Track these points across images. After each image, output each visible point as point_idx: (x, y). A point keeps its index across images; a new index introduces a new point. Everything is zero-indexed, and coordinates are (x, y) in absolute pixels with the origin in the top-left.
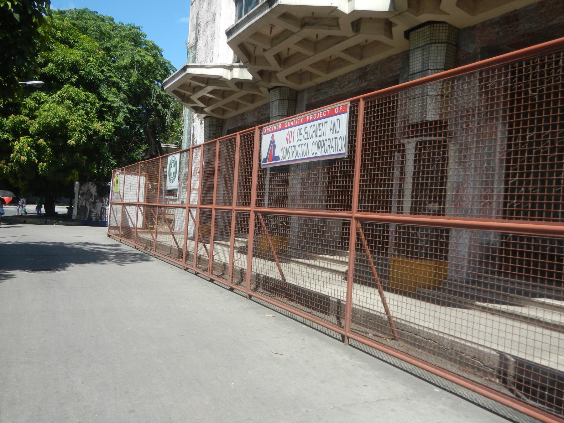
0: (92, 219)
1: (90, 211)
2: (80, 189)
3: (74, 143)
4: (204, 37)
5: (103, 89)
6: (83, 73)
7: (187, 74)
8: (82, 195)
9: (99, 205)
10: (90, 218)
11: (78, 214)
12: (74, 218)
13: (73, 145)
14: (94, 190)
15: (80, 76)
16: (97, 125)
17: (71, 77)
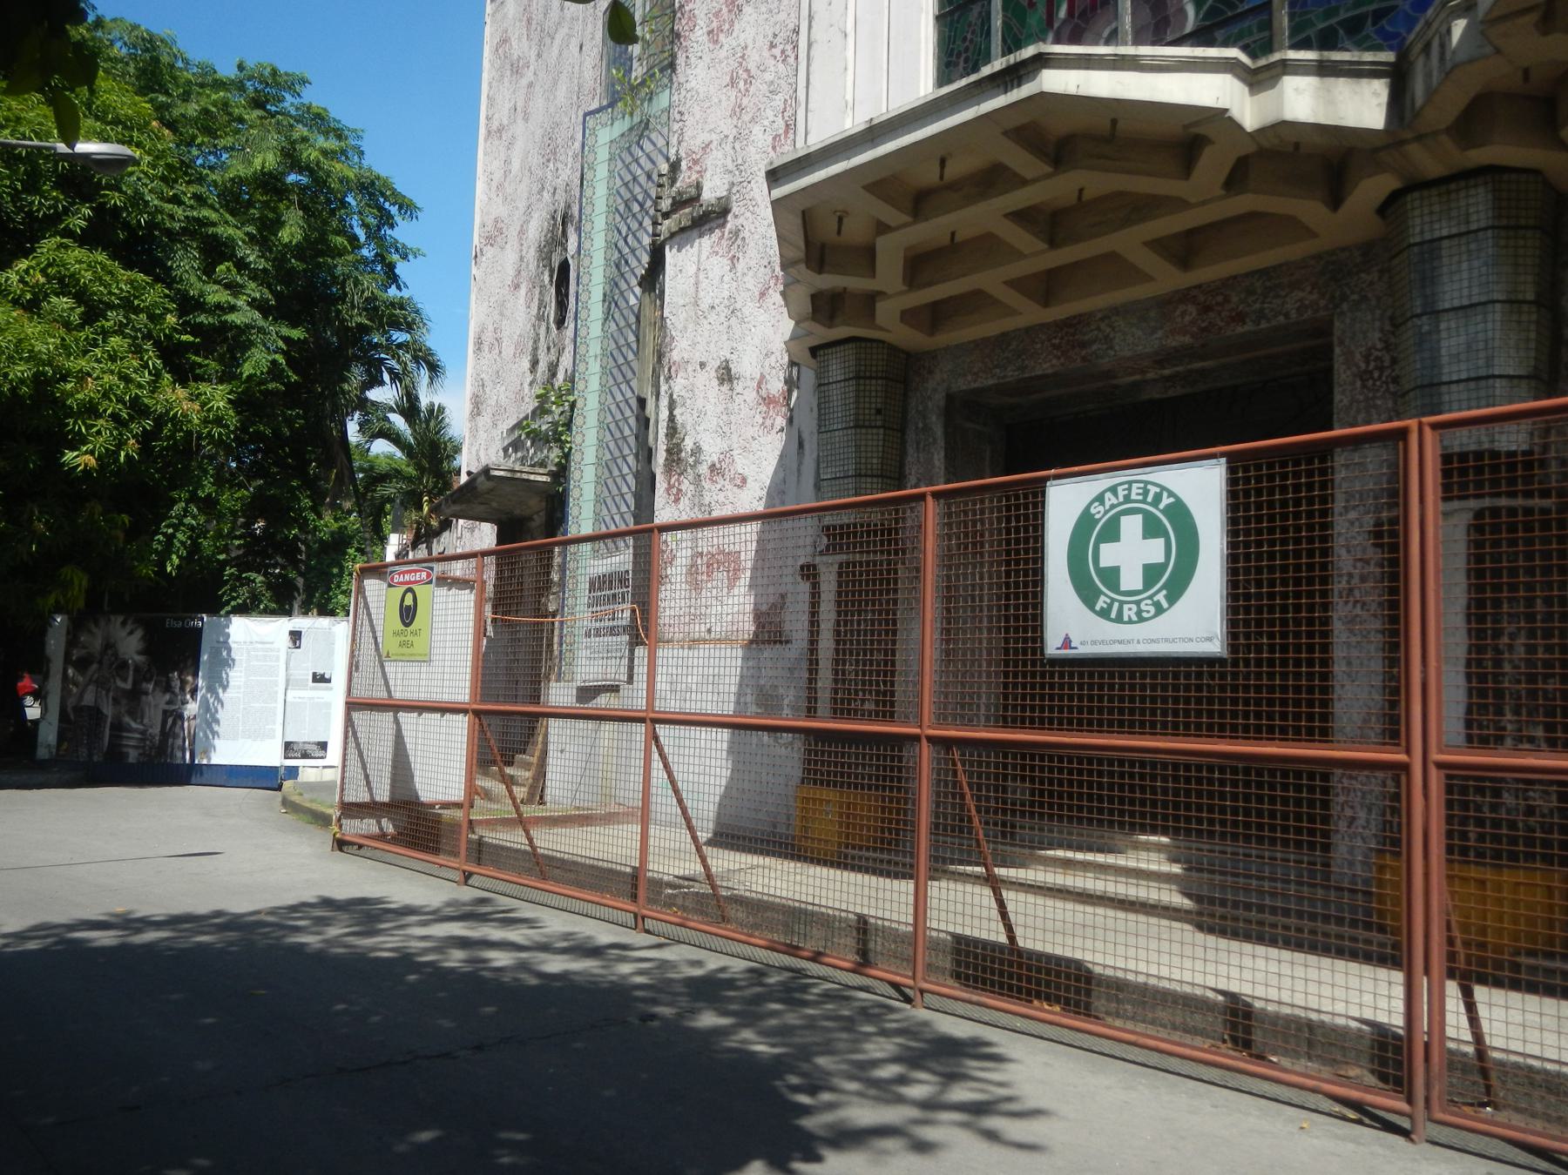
0: (125, 755)
1: (118, 727)
2: (72, 642)
3: (92, 462)
4: (723, 53)
5: (185, 263)
6: (116, 199)
7: (1043, 96)
8: (82, 664)
9: (156, 702)
10: (115, 753)
11: (61, 736)
12: (42, 753)
13: (87, 472)
14: (131, 645)
15: (100, 210)
16: (176, 398)
17: (66, 211)
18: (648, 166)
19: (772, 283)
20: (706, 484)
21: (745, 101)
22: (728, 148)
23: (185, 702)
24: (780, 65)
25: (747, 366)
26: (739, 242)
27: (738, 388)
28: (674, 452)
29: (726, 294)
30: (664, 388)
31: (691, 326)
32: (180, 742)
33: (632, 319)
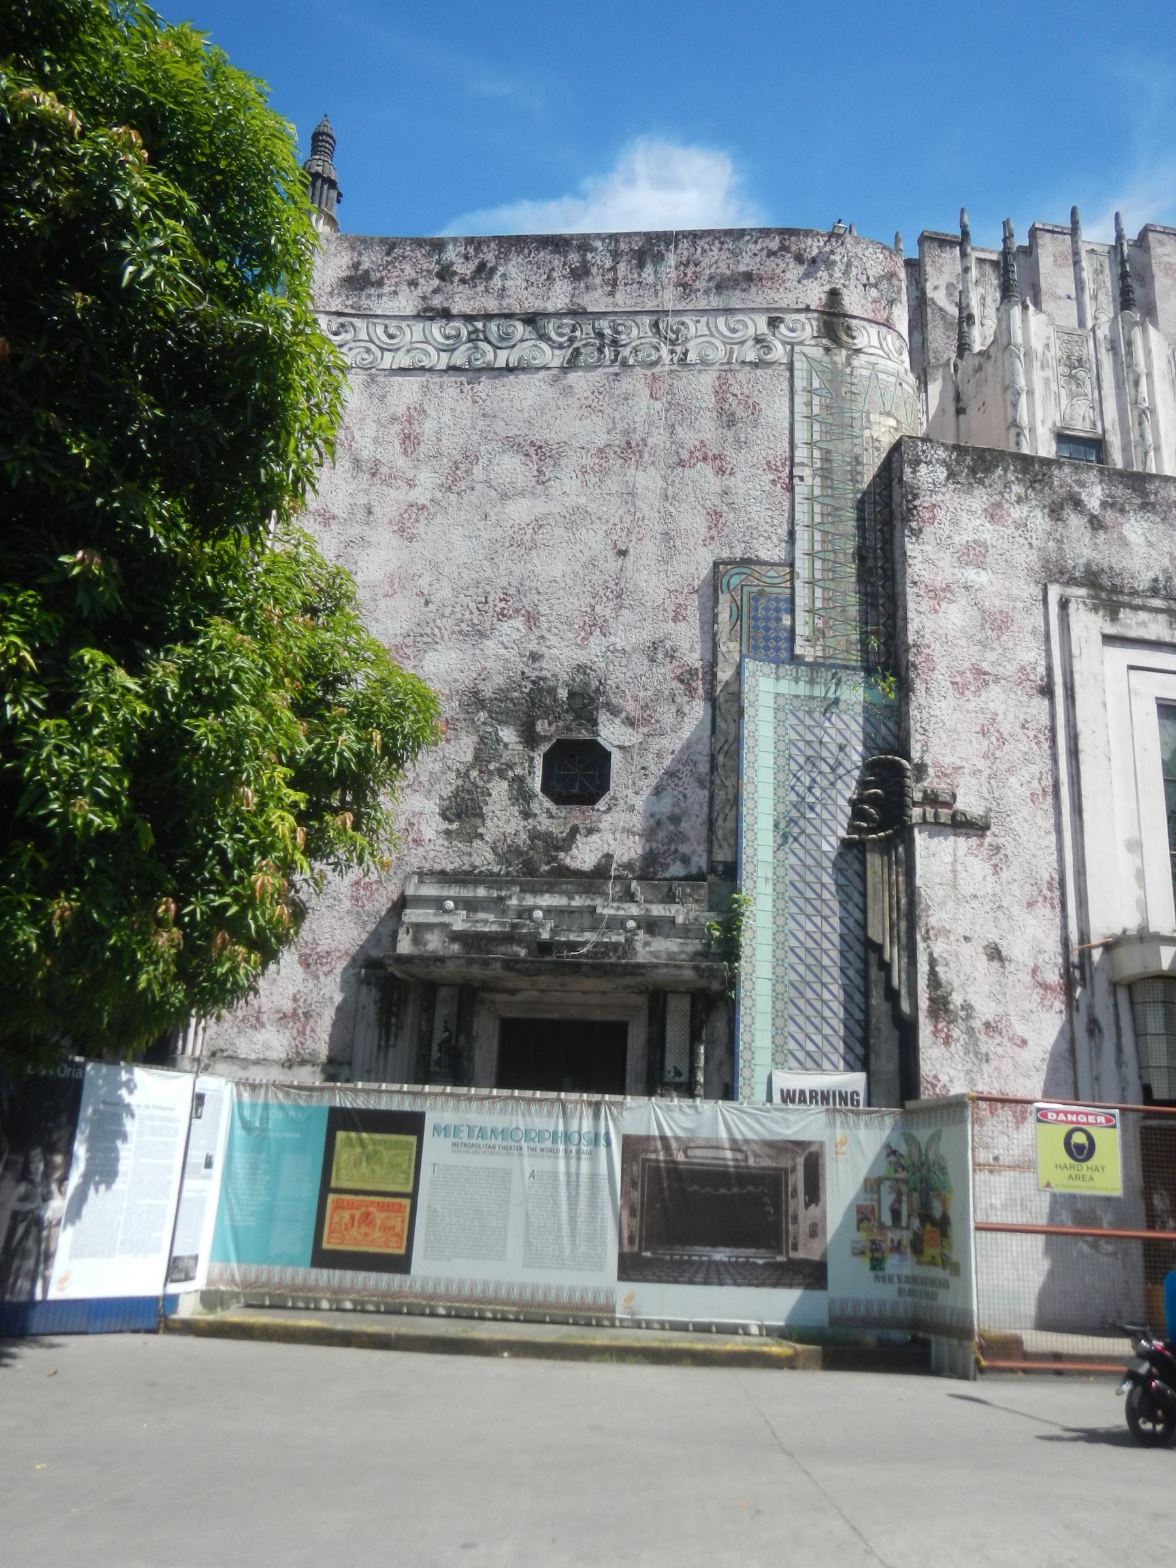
18: (840, 740)
19: (1040, 899)
20: (983, 1038)
21: (998, 754)
22: (983, 780)
23: (47, 1197)
24: (1035, 747)
25: (1018, 950)
26: (1000, 855)
27: (1011, 968)
28: (940, 1006)
29: (990, 891)
30: (921, 946)
31: (950, 905)
32: (30, 1264)
33: (827, 864)
